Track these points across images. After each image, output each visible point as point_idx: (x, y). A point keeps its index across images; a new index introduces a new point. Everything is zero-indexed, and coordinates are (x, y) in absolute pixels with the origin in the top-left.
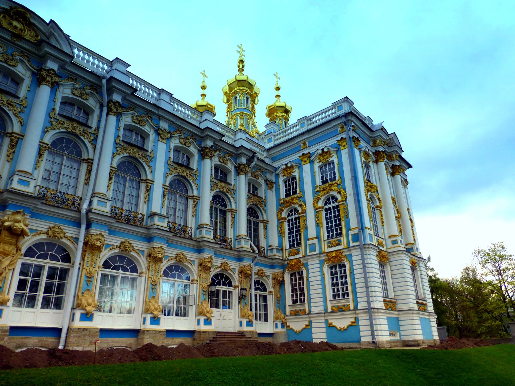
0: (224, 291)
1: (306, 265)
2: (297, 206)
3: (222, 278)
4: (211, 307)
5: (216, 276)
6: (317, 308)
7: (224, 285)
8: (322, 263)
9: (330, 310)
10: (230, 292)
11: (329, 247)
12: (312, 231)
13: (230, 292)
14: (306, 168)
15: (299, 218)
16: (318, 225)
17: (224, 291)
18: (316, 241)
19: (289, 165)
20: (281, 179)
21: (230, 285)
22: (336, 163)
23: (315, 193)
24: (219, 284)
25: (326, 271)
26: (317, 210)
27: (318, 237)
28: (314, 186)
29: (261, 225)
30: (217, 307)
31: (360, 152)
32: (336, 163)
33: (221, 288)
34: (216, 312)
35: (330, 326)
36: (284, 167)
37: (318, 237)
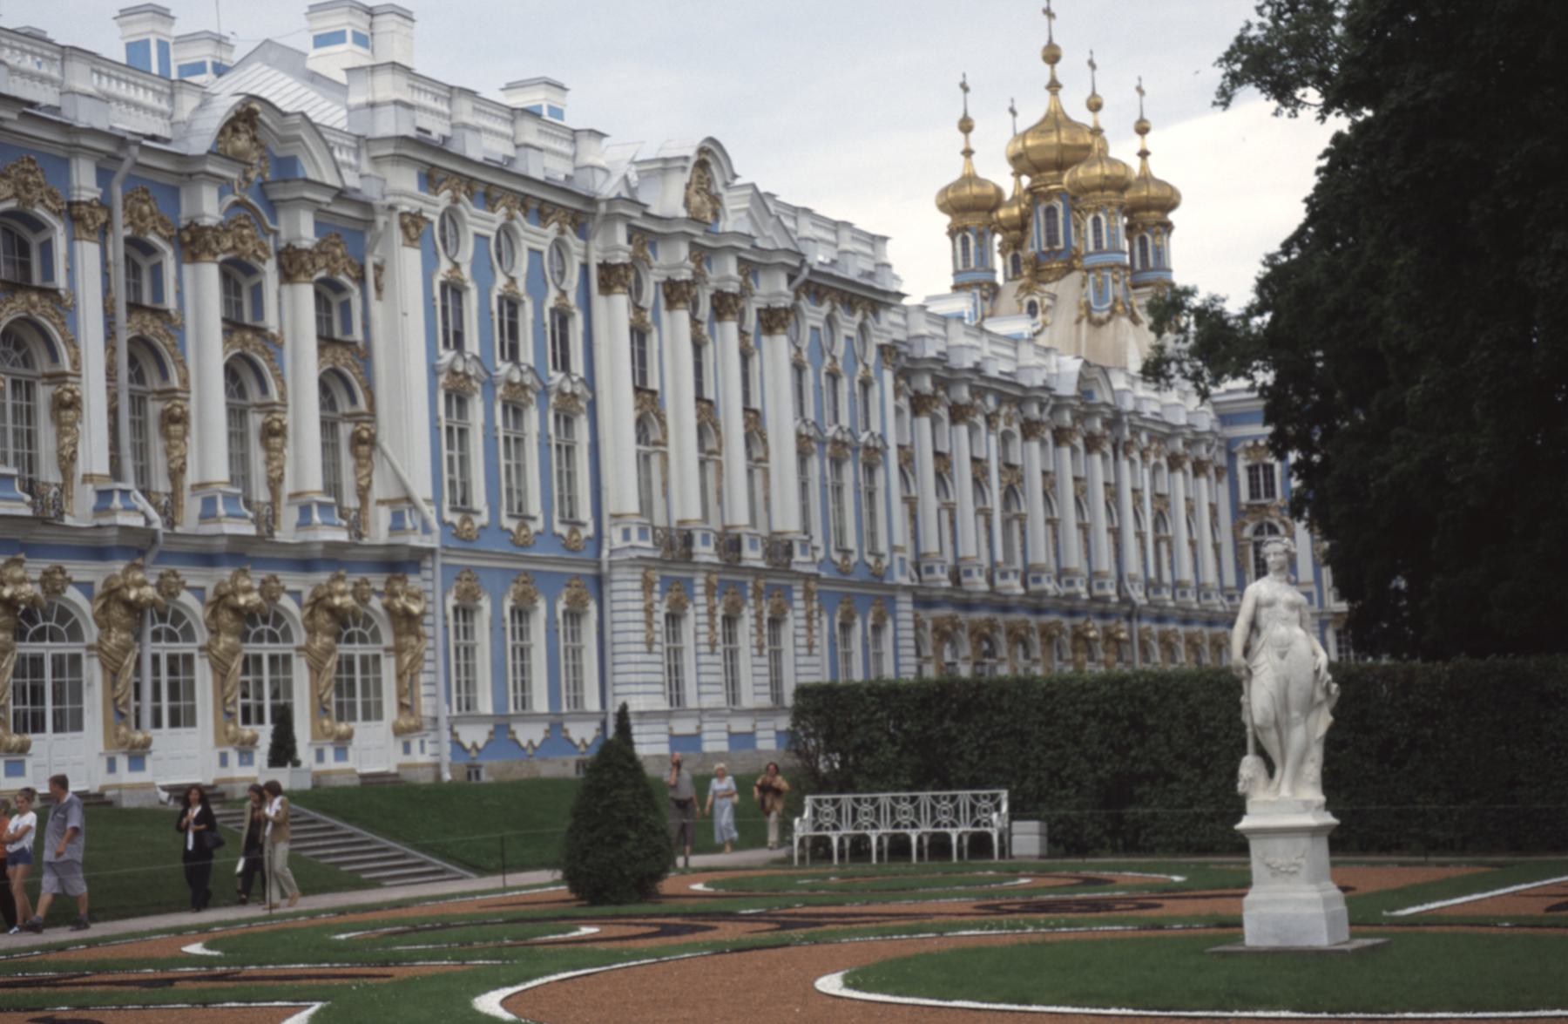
2: (1275, 522)
18: (1314, 589)
20: (1242, 465)
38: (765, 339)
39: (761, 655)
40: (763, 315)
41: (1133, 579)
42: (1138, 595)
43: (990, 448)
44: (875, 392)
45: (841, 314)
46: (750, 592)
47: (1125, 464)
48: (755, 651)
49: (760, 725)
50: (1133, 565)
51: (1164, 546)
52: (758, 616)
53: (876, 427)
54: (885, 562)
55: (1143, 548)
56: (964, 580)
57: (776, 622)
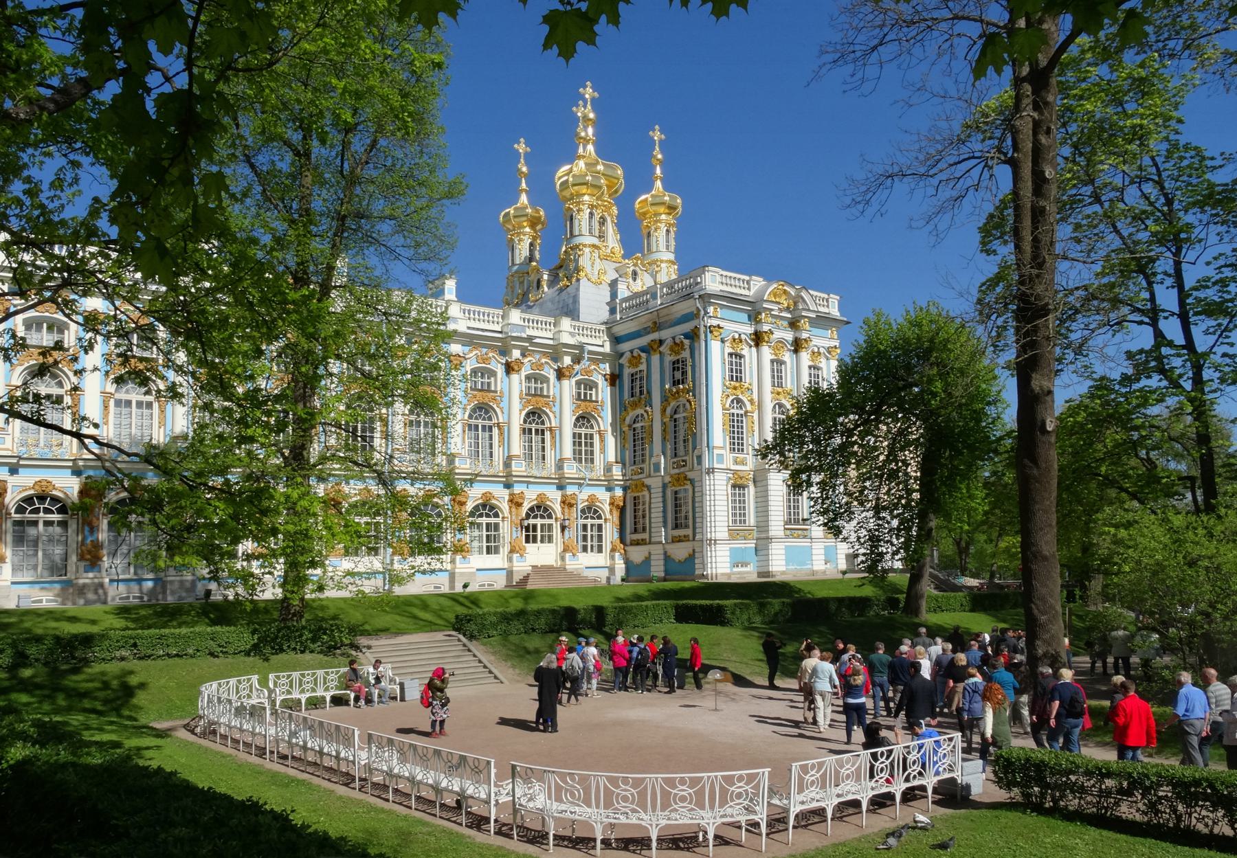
0: (542, 525)
3: (540, 509)
4: (527, 541)
5: (531, 509)
7: (542, 517)
10: (550, 526)
13: (550, 526)
14: (655, 358)
16: (664, 439)
17: (542, 525)
19: (635, 354)
21: (550, 517)
24: (535, 517)
29: (596, 438)
30: (535, 541)
31: (723, 341)
33: (539, 522)
34: (530, 547)
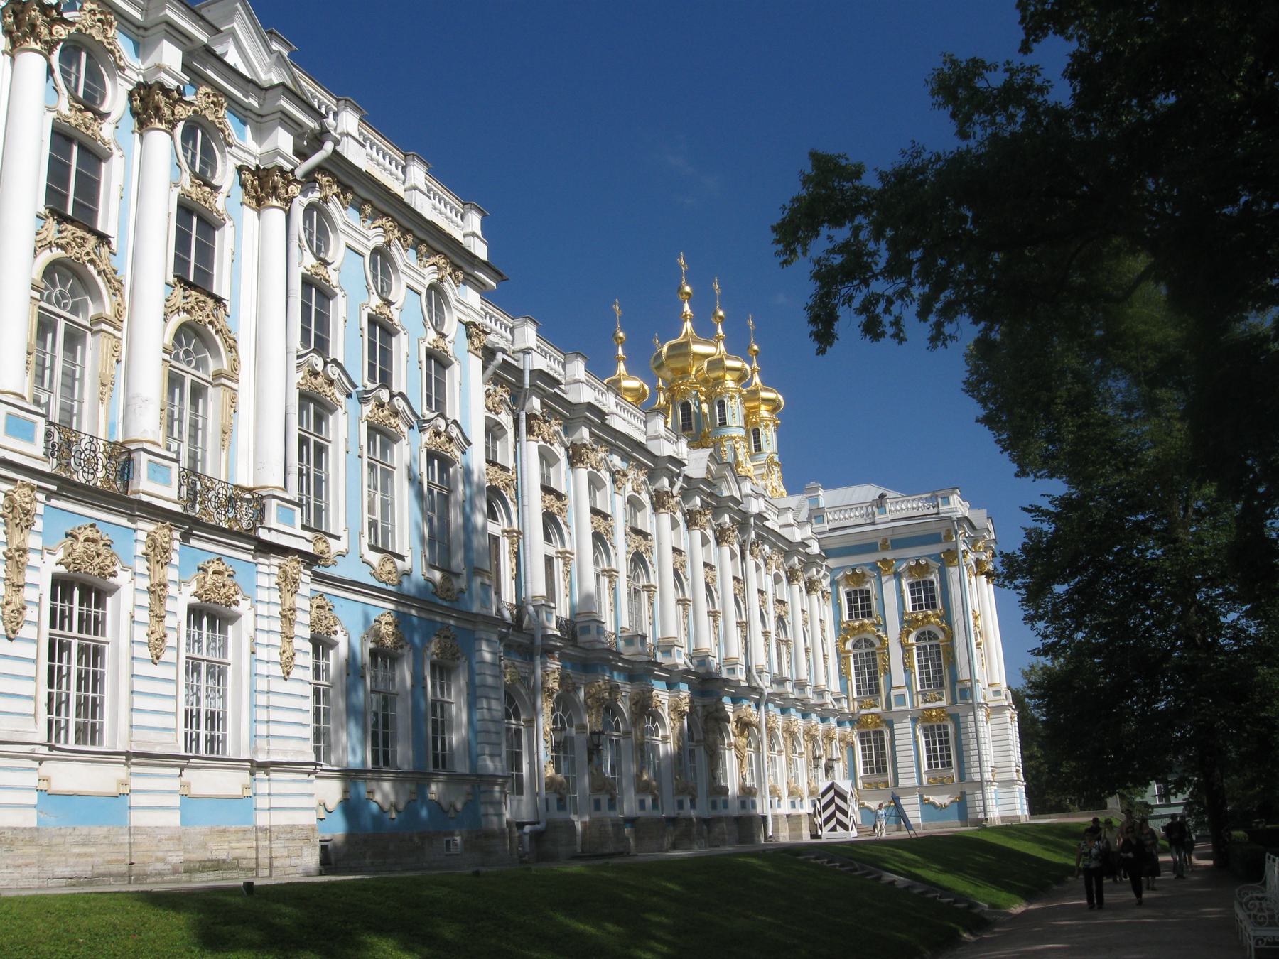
1: (890, 724)
2: (869, 637)
6: (907, 779)
8: (915, 721)
9: (925, 783)
11: (925, 701)
12: (898, 676)
15: (873, 654)
16: (908, 670)
22: (937, 585)
23: (902, 621)
25: (920, 734)
26: (906, 649)
27: (909, 685)
28: (902, 612)
32: (937, 585)
35: (925, 803)
36: (849, 573)
37: (909, 685)
38: (249, 214)
39: (156, 660)
40: (247, 176)
41: (760, 672)
42: (765, 683)
43: (616, 505)
44: (453, 376)
45: (403, 257)
46: (141, 549)
47: (751, 563)
48: (144, 652)
49: (136, 783)
50: (759, 658)
51: (783, 648)
52: (158, 592)
53: (453, 412)
54: (461, 583)
55: (767, 645)
56: (582, 639)
57: (211, 615)
